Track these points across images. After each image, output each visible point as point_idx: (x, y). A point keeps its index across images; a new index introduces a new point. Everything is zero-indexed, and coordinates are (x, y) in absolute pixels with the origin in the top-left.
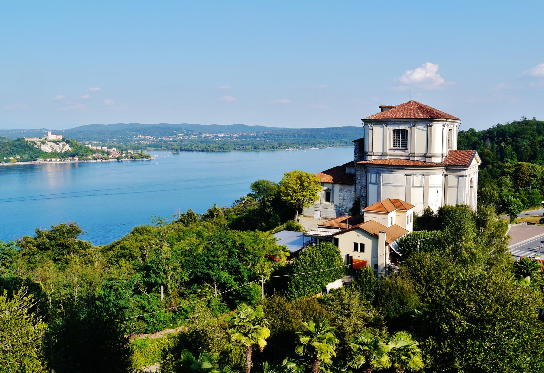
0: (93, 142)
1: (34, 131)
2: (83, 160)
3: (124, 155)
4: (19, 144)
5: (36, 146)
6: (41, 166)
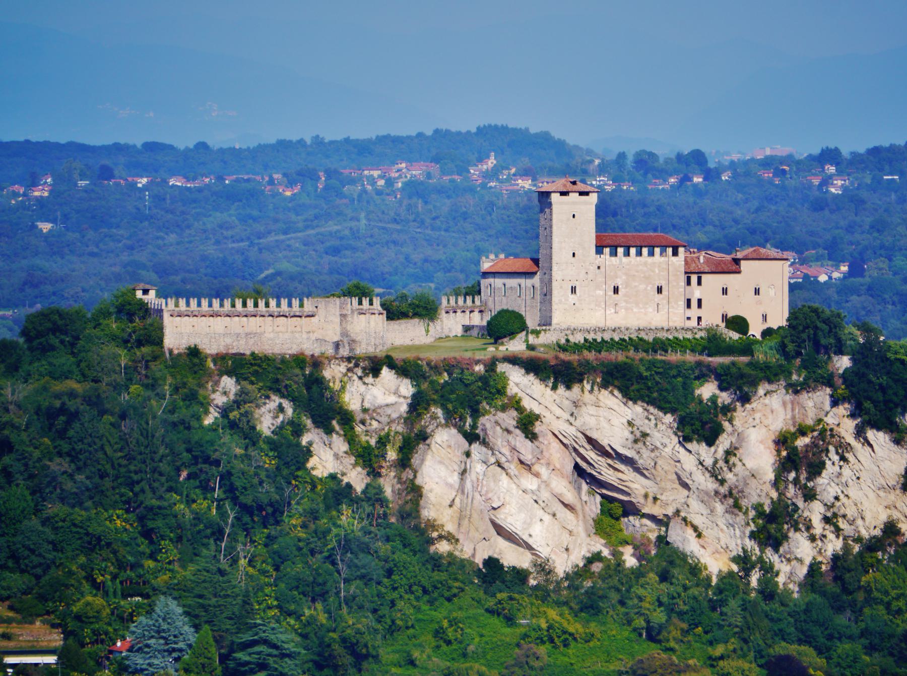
5: (327, 457)
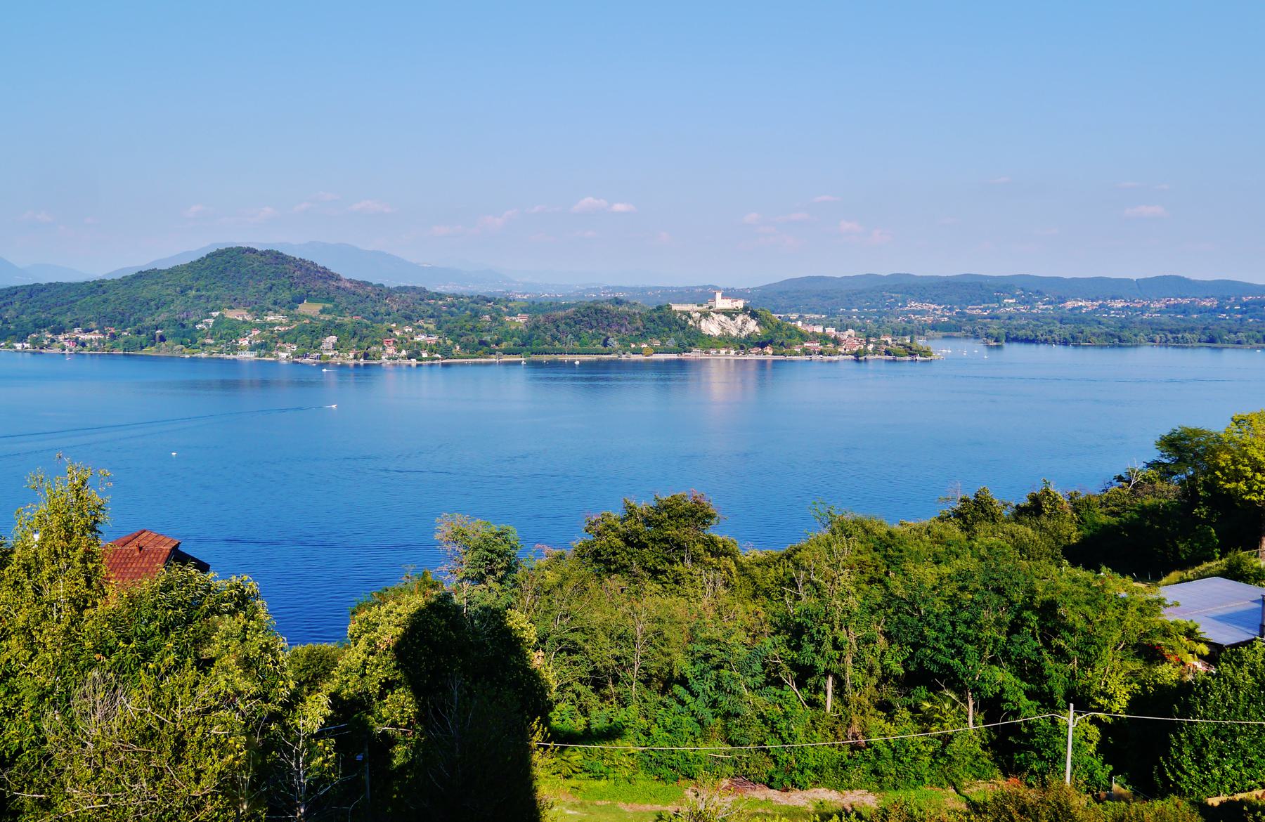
0: (807, 316)
1: (690, 290)
3: (870, 347)
4: (660, 318)
5: (690, 322)
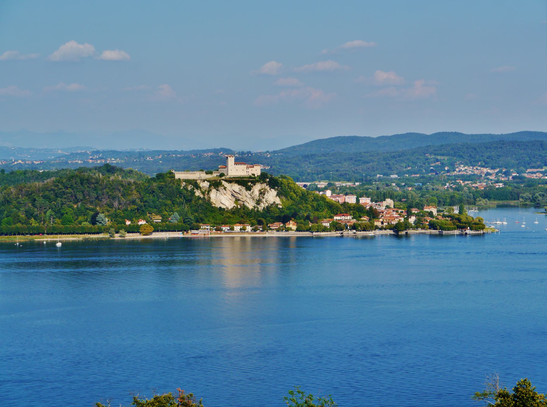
0: (338, 184)
1: (198, 154)
2: (309, 230)
3: (412, 220)
4: (161, 188)
5: (198, 193)
6: (210, 243)
